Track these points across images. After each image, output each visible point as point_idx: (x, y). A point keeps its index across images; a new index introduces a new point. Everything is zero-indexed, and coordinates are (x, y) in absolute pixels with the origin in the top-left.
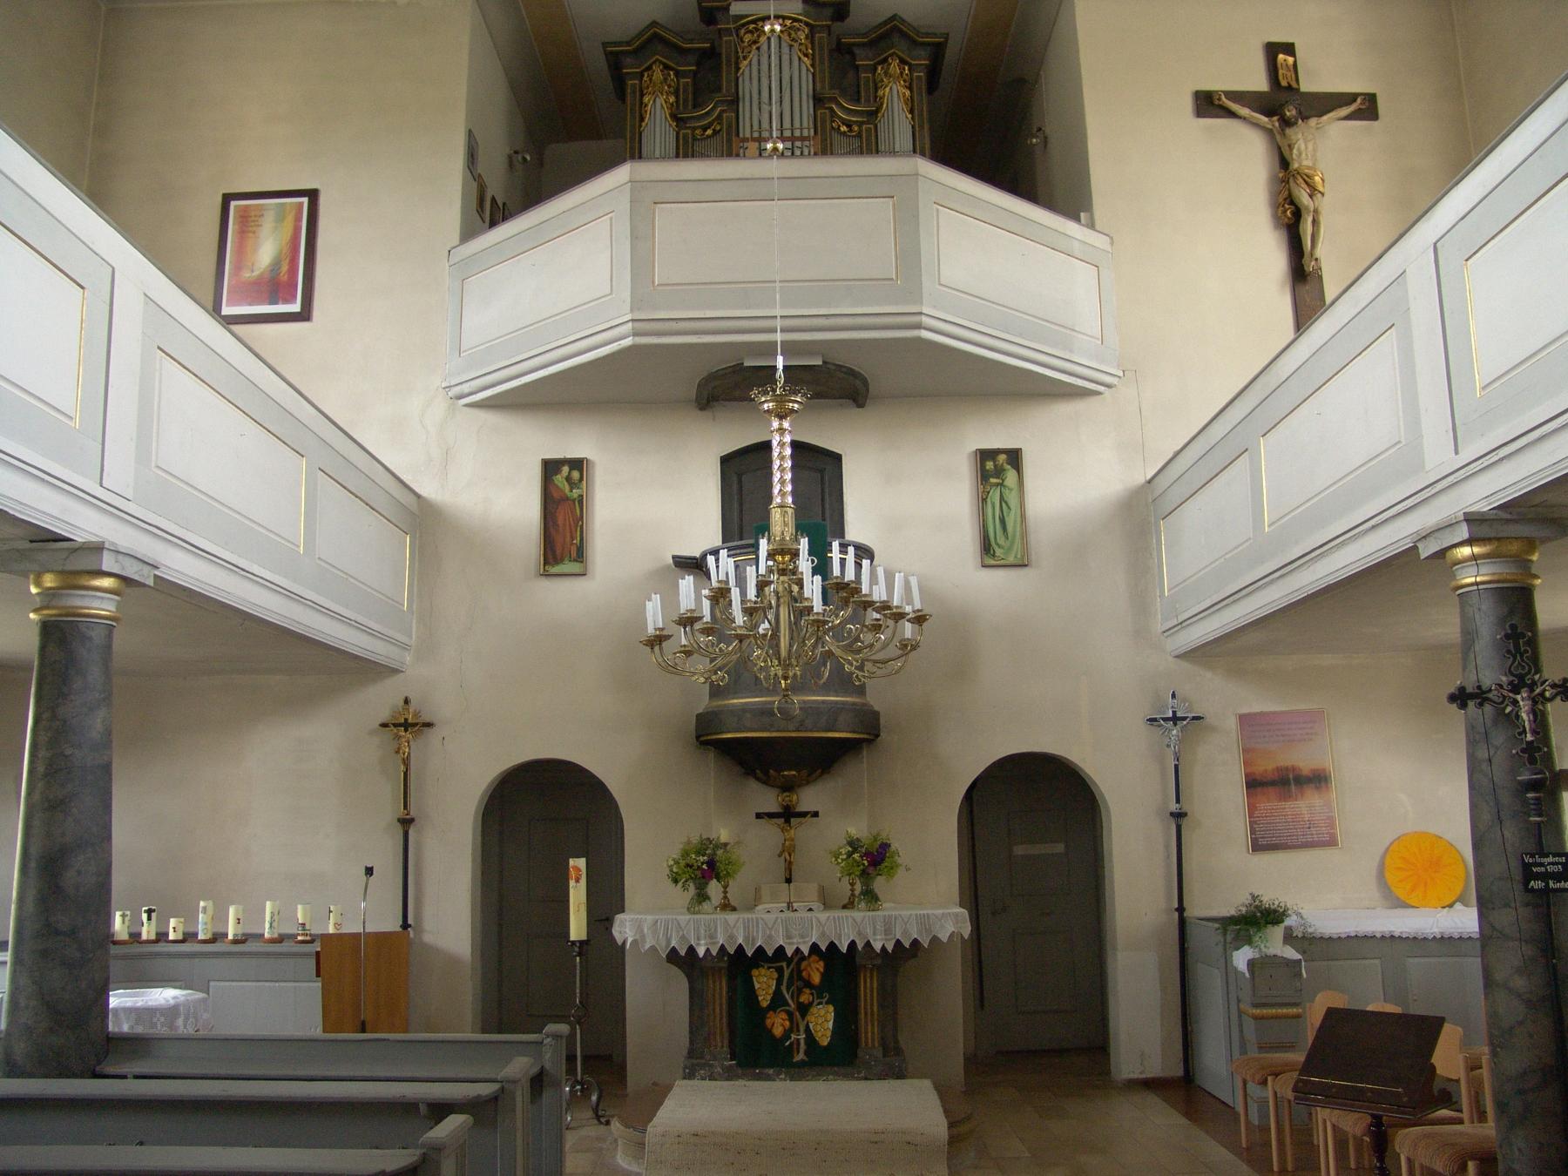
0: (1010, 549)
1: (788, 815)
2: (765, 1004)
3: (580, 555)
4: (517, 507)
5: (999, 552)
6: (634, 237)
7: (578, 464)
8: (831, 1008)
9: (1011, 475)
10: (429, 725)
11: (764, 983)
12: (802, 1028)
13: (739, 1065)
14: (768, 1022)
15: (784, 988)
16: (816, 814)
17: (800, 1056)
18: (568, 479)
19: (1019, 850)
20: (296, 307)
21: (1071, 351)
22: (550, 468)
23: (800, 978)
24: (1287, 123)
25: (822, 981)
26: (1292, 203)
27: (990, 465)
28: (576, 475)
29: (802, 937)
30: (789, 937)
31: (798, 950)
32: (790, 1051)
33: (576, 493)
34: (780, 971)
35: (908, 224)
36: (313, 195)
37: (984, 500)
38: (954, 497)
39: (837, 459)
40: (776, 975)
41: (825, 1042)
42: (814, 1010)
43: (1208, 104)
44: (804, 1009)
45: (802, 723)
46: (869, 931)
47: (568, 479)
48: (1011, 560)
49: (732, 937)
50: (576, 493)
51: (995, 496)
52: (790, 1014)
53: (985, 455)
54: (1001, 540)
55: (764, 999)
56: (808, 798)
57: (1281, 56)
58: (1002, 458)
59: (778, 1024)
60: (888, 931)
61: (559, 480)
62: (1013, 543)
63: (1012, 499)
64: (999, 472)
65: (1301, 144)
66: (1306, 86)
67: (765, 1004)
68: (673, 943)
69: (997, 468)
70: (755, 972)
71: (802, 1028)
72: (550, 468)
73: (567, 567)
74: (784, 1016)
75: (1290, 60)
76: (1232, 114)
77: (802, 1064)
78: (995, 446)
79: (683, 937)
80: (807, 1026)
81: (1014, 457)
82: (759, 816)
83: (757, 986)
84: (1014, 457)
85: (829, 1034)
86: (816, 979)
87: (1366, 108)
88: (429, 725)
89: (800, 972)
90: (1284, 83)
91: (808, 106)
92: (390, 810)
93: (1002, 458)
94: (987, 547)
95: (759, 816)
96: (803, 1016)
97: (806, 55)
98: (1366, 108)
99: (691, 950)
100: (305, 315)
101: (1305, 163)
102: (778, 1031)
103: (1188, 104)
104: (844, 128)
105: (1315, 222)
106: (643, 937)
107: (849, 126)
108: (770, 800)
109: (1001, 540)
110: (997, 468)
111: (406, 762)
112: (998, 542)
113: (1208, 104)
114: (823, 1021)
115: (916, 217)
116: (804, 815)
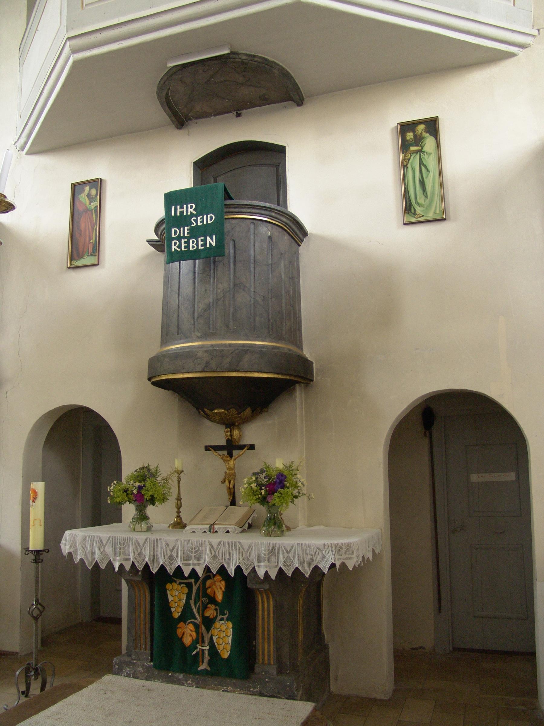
0: (430, 205)
1: (231, 448)
2: (176, 615)
5: (419, 210)
7: (97, 184)
8: (230, 625)
9: (429, 143)
11: (176, 596)
12: (207, 640)
13: (155, 666)
14: (179, 631)
15: (192, 602)
16: (252, 447)
17: (203, 666)
18: (89, 196)
19: (475, 478)
21: (477, 12)
22: (76, 188)
23: (205, 595)
25: (223, 598)
27: (410, 136)
29: (197, 559)
30: (186, 558)
31: (193, 572)
32: (196, 660)
34: (189, 586)
37: (405, 167)
40: (186, 590)
41: (225, 655)
42: (217, 625)
44: (209, 623)
45: (207, 363)
46: (254, 558)
48: (430, 215)
49: (140, 555)
51: (415, 161)
52: (197, 626)
53: (405, 127)
54: (421, 200)
55: (176, 612)
56: (251, 433)
59: (188, 633)
60: (271, 559)
61: (83, 197)
62: (432, 201)
64: (418, 140)
67: (176, 615)
68: (97, 558)
70: (169, 586)
71: (207, 640)
74: (191, 627)
77: (205, 673)
79: (104, 552)
80: (211, 638)
81: (432, 125)
82: (207, 448)
83: (170, 598)
84: (432, 125)
85: (229, 648)
86: (219, 597)
89: (205, 589)
94: (408, 207)
95: (207, 448)
96: (208, 630)
99: (110, 565)
102: (187, 641)
106: (76, 551)
108: (218, 435)
109: (421, 200)
110: (418, 136)
112: (419, 203)
114: (224, 635)
116: (242, 447)
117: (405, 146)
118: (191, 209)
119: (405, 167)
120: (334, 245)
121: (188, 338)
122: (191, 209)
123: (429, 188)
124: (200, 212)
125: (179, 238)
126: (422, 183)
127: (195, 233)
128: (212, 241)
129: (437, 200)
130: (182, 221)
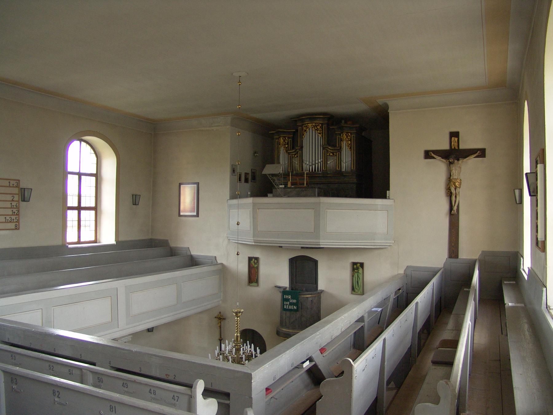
3: (257, 281)
4: (243, 268)
6: (253, 218)
7: (257, 259)
9: (361, 270)
10: (225, 319)
20: (195, 214)
21: (374, 240)
22: (250, 259)
24: (451, 163)
26: (450, 190)
27: (355, 266)
28: (256, 261)
33: (256, 266)
35: (317, 216)
36: (198, 184)
38: (345, 274)
39: (316, 262)
43: (428, 155)
47: (254, 262)
48: (359, 292)
50: (256, 266)
51: (356, 275)
53: (354, 264)
54: (357, 287)
57: (453, 138)
58: (359, 265)
61: (252, 262)
64: (357, 269)
66: (461, 147)
69: (357, 267)
72: (250, 259)
73: (254, 284)
75: (456, 139)
78: (356, 261)
81: (362, 265)
84: (362, 265)
87: (481, 153)
88: (225, 319)
90: (453, 147)
91: (320, 149)
92: (218, 337)
93: (359, 265)
94: (353, 289)
97: (320, 133)
98: (481, 153)
100: (198, 215)
101: (454, 177)
103: (422, 154)
104: (331, 154)
105: (456, 197)
107: (333, 153)
109: (357, 287)
110: (357, 267)
113: (428, 155)
117: (353, 269)
118: (290, 297)
119: (353, 276)
121: (288, 328)
122: (290, 297)
124: (292, 298)
125: (286, 305)
126: (358, 282)
127: (291, 304)
128: (295, 307)
129: (361, 288)
130: (287, 300)
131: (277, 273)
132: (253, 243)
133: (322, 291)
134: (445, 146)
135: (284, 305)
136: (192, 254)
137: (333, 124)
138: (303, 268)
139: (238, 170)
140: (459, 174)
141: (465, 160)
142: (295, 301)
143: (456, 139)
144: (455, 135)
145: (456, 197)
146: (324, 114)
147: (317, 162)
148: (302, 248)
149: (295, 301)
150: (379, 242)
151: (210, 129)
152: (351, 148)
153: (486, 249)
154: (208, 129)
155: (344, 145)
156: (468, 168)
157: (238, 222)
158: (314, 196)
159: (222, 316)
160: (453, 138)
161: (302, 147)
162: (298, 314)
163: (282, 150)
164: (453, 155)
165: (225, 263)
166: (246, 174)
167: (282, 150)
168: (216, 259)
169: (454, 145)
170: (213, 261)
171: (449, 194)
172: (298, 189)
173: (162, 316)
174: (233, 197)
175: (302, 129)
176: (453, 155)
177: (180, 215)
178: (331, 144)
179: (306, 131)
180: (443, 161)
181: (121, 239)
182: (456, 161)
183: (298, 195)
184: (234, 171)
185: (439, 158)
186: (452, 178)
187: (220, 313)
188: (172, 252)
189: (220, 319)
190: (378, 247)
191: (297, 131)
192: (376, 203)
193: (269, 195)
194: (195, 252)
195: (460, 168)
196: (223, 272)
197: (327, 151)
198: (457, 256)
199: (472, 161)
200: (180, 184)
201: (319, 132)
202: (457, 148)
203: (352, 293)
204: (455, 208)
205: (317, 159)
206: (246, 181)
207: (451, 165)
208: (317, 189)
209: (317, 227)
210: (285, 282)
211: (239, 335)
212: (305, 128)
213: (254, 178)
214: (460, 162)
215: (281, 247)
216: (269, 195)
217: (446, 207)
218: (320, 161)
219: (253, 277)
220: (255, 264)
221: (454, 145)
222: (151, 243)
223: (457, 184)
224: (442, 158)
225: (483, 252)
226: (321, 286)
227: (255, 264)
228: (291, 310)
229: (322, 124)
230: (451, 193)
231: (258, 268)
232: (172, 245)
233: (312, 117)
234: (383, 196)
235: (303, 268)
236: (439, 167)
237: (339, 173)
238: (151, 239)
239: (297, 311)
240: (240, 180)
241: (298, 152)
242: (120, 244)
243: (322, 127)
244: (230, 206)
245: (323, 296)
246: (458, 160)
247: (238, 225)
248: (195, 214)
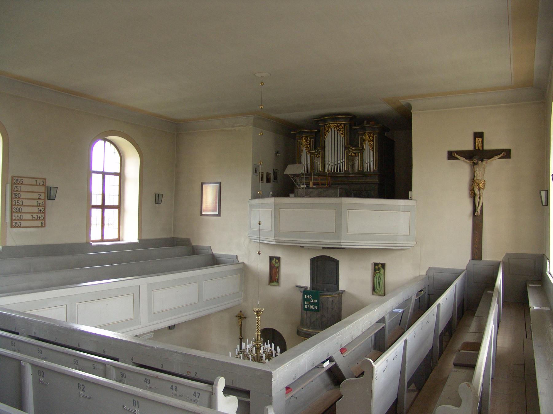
3: (278, 281)
4: (264, 267)
7: (278, 258)
9: (382, 271)
10: (245, 318)
20: (217, 213)
22: (271, 258)
24: (474, 164)
27: (377, 267)
28: (277, 261)
33: (277, 265)
35: (339, 216)
36: (220, 184)
38: (367, 275)
39: (337, 263)
43: (451, 155)
48: (381, 293)
50: (277, 265)
51: (377, 276)
53: (375, 264)
54: (378, 288)
57: (477, 139)
58: (380, 265)
61: (273, 261)
63: (382, 277)
64: (379, 269)
65: (478, 172)
66: (486, 147)
69: (379, 268)
73: (275, 283)
75: (480, 140)
76: (457, 159)
78: (378, 262)
81: (383, 265)
84: (383, 265)
87: (507, 154)
88: (245, 318)
90: (477, 148)
91: (342, 150)
92: (239, 336)
93: (380, 265)
94: (374, 290)
97: (342, 134)
98: (507, 154)
100: (219, 215)
101: (478, 178)
103: (445, 155)
104: (353, 155)
105: (479, 198)
107: (355, 153)
110: (379, 268)
111: (241, 326)
113: (451, 155)
115: (341, 215)
117: (375, 270)
118: (310, 297)
119: (374, 277)
120: (352, 296)
121: (308, 328)
122: (310, 297)
123: (381, 285)
124: (313, 298)
126: (379, 283)
127: (312, 304)
129: (383, 289)
130: (308, 300)
131: (298, 273)
132: (275, 243)
133: (343, 292)
134: (470, 147)
135: (304, 305)
136: (214, 252)
137: (355, 125)
138: (324, 269)
139: (260, 170)
140: (483, 175)
141: (489, 161)
142: (315, 301)
143: (480, 140)
144: (479, 135)
145: (479, 198)
146: (347, 114)
147: (339, 162)
148: (323, 248)
149: (315, 301)
150: (401, 243)
151: (233, 129)
152: (373, 148)
153: (511, 250)
154: (230, 129)
155: (366, 144)
156: (492, 169)
157: (260, 222)
158: (335, 196)
159: (243, 315)
160: (477, 139)
161: (324, 147)
162: (319, 315)
163: (304, 150)
164: (477, 155)
165: (246, 262)
166: (268, 174)
167: (304, 150)
168: (237, 258)
169: (478, 145)
170: (234, 260)
171: (473, 195)
172: (320, 190)
173: (184, 314)
174: (255, 196)
175: (325, 129)
176: (477, 155)
177: (202, 215)
178: (353, 144)
179: (328, 131)
180: (466, 162)
181: (143, 237)
182: (480, 162)
183: (320, 195)
184: (256, 171)
185: (463, 159)
186: (475, 179)
187: (241, 312)
188: (194, 251)
189: (241, 317)
190: (400, 248)
191: (319, 131)
192: (399, 204)
193: (291, 195)
194: (216, 251)
195: (484, 169)
196: (244, 271)
197: (349, 151)
198: (480, 258)
199: (496, 162)
200: (202, 184)
201: (341, 132)
202: (481, 149)
203: (373, 294)
204: (479, 209)
205: (339, 159)
206: (268, 181)
207: (475, 166)
208: (338, 190)
209: (339, 227)
210: (306, 282)
211: (259, 334)
212: (327, 129)
213: (275, 178)
214: (484, 163)
215: (303, 247)
216: (291, 195)
217: (470, 208)
218: (342, 161)
219: (274, 276)
220: (276, 263)
221: (478, 145)
222: (173, 242)
223: (481, 185)
224: (466, 159)
225: (507, 254)
226: (342, 286)
227: (276, 263)
228: (312, 310)
229: (345, 125)
230: (475, 194)
231: (279, 268)
232: (194, 244)
233: (334, 117)
234: (406, 196)
235: (324, 269)
236: (463, 168)
237: (362, 174)
238: (173, 238)
239: (318, 310)
240: (262, 180)
241: (319, 153)
242: (143, 243)
243: (344, 127)
244: (252, 206)
245: (344, 298)
246: (482, 161)
247: (260, 224)
248: (217, 213)
